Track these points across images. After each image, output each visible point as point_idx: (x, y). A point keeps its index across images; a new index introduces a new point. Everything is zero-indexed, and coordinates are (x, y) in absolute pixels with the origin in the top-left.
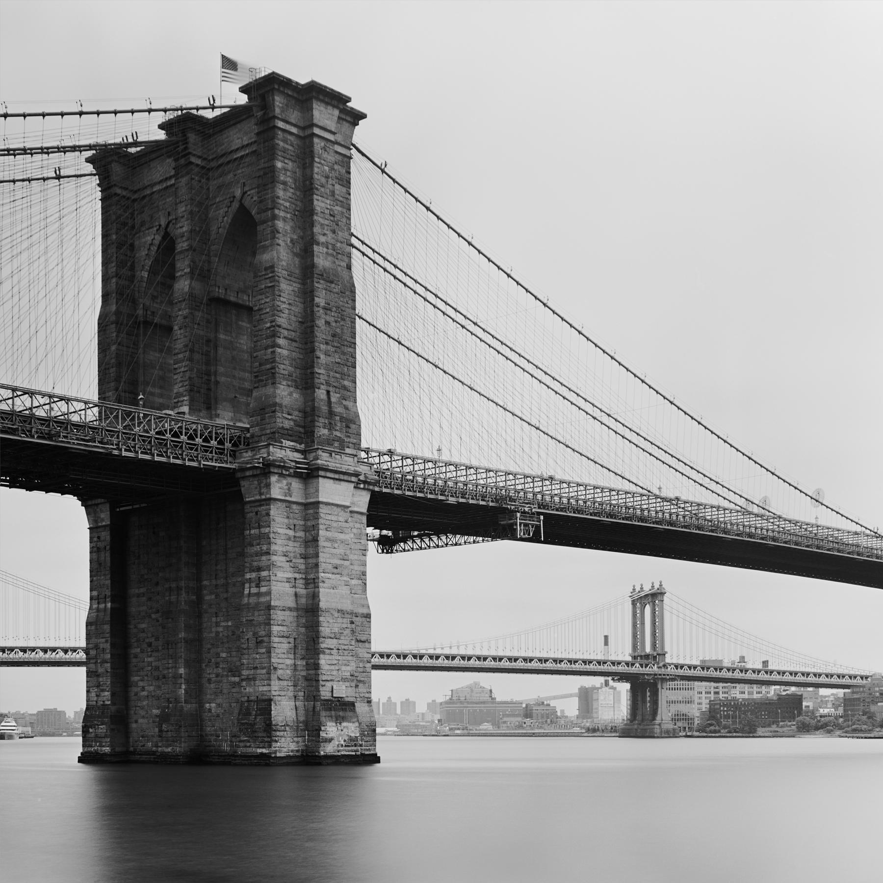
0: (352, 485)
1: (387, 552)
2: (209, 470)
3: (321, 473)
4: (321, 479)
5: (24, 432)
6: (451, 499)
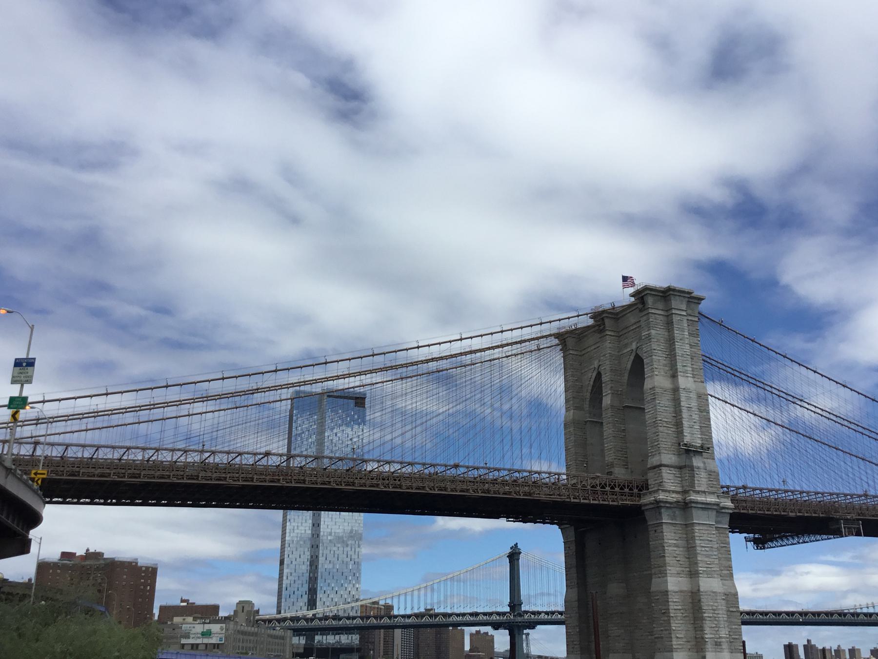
0: (714, 513)
1: (761, 549)
2: (625, 507)
3: (693, 505)
4: (693, 508)
5: (515, 493)
6: (790, 514)
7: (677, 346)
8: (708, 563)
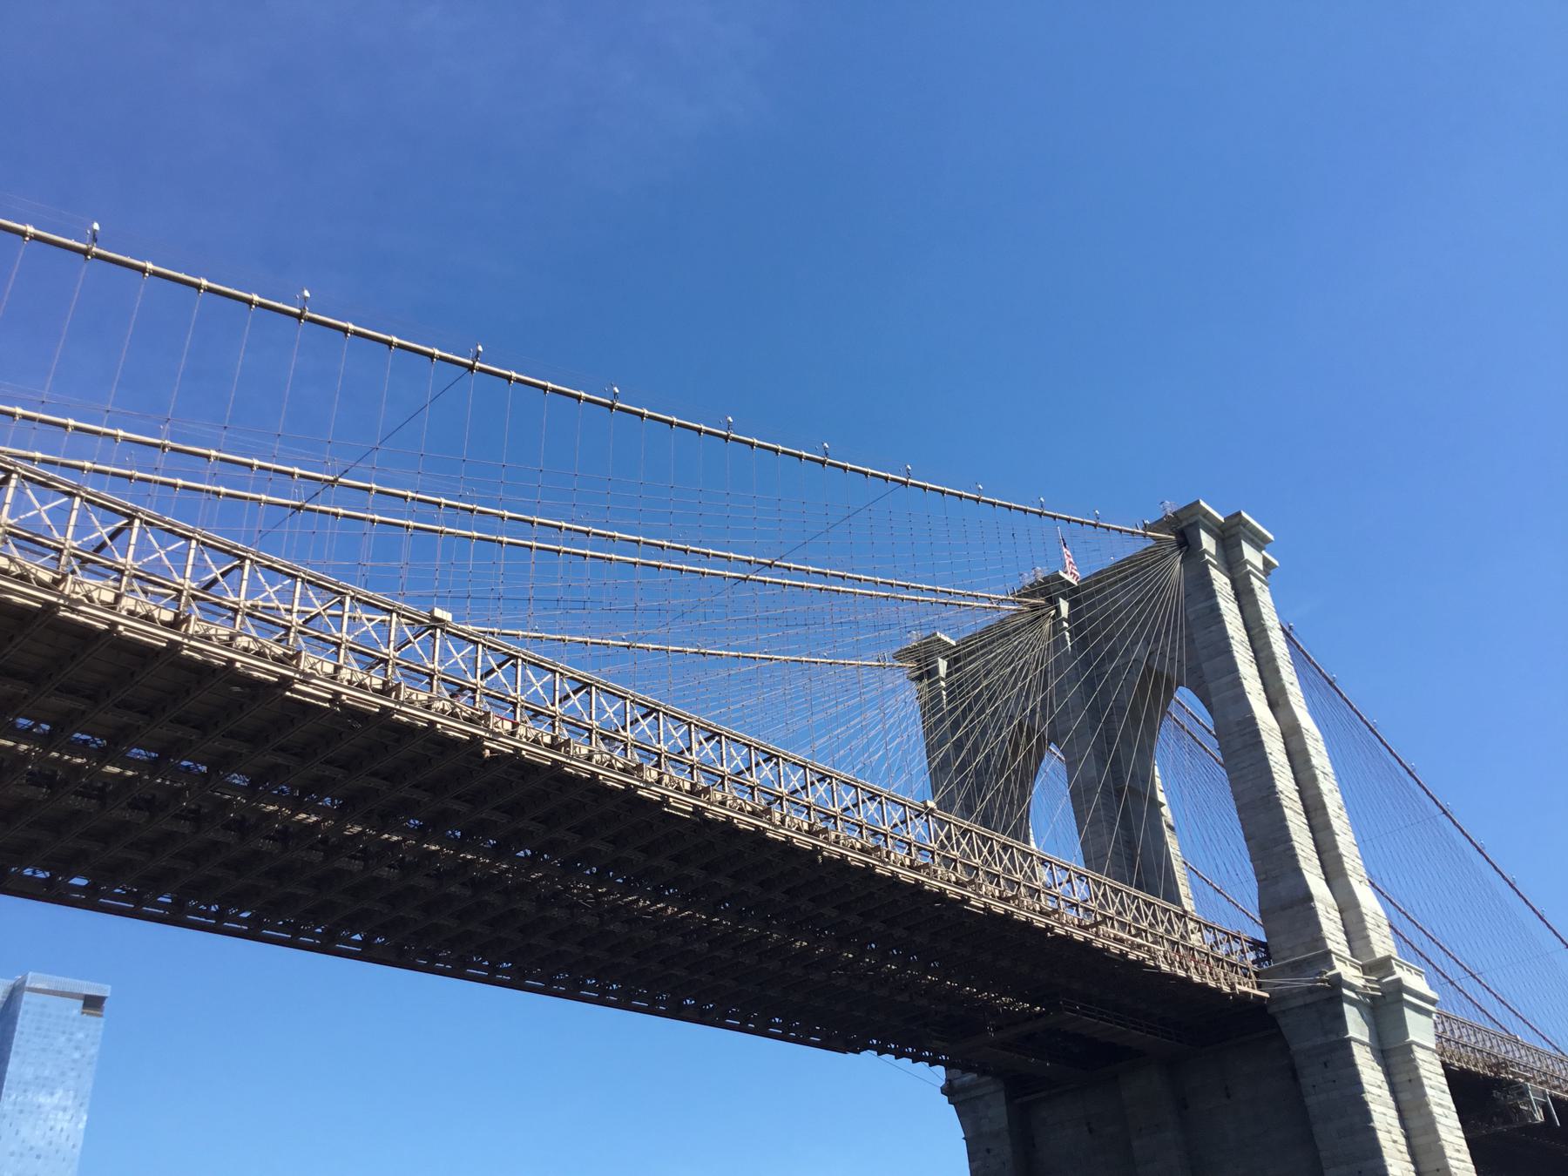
3: (1406, 996)
7: (1272, 640)
8: (1457, 1147)
